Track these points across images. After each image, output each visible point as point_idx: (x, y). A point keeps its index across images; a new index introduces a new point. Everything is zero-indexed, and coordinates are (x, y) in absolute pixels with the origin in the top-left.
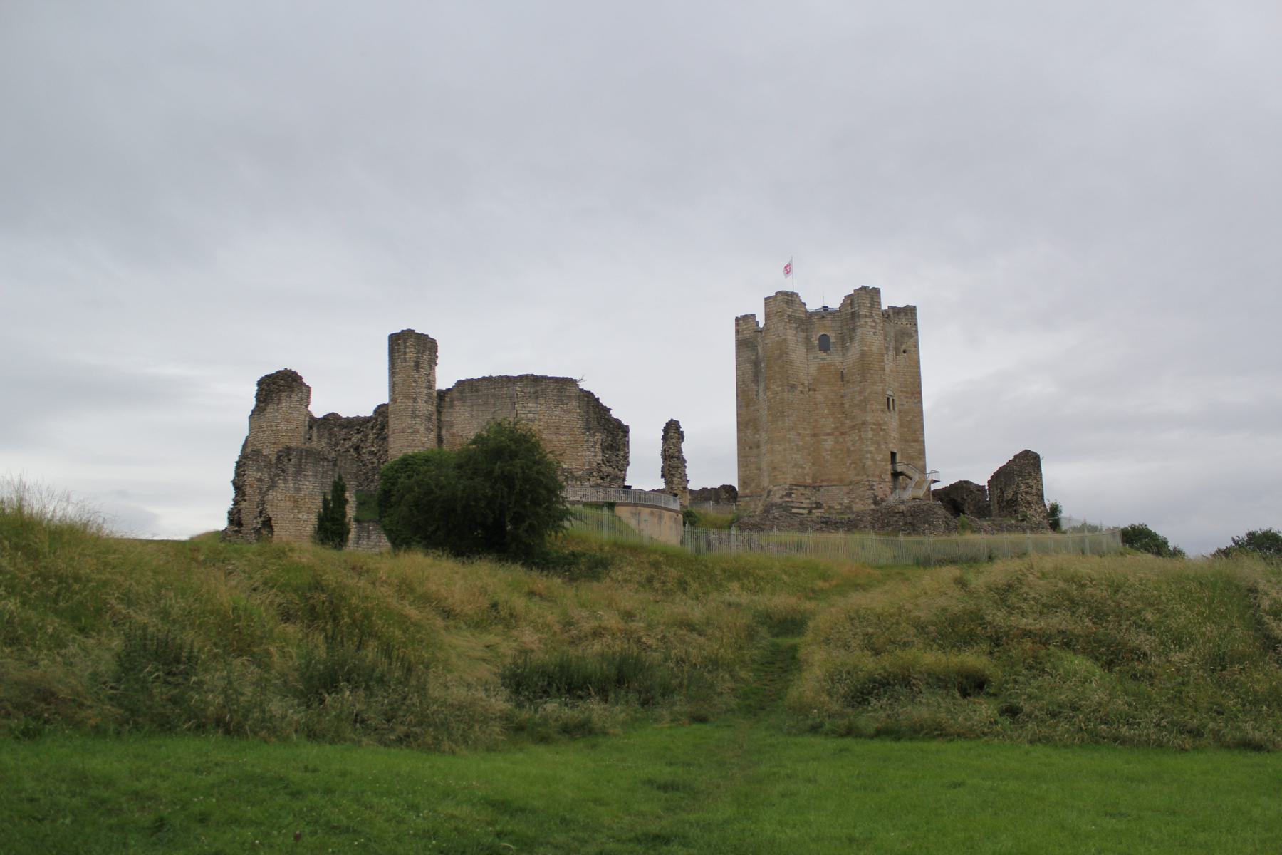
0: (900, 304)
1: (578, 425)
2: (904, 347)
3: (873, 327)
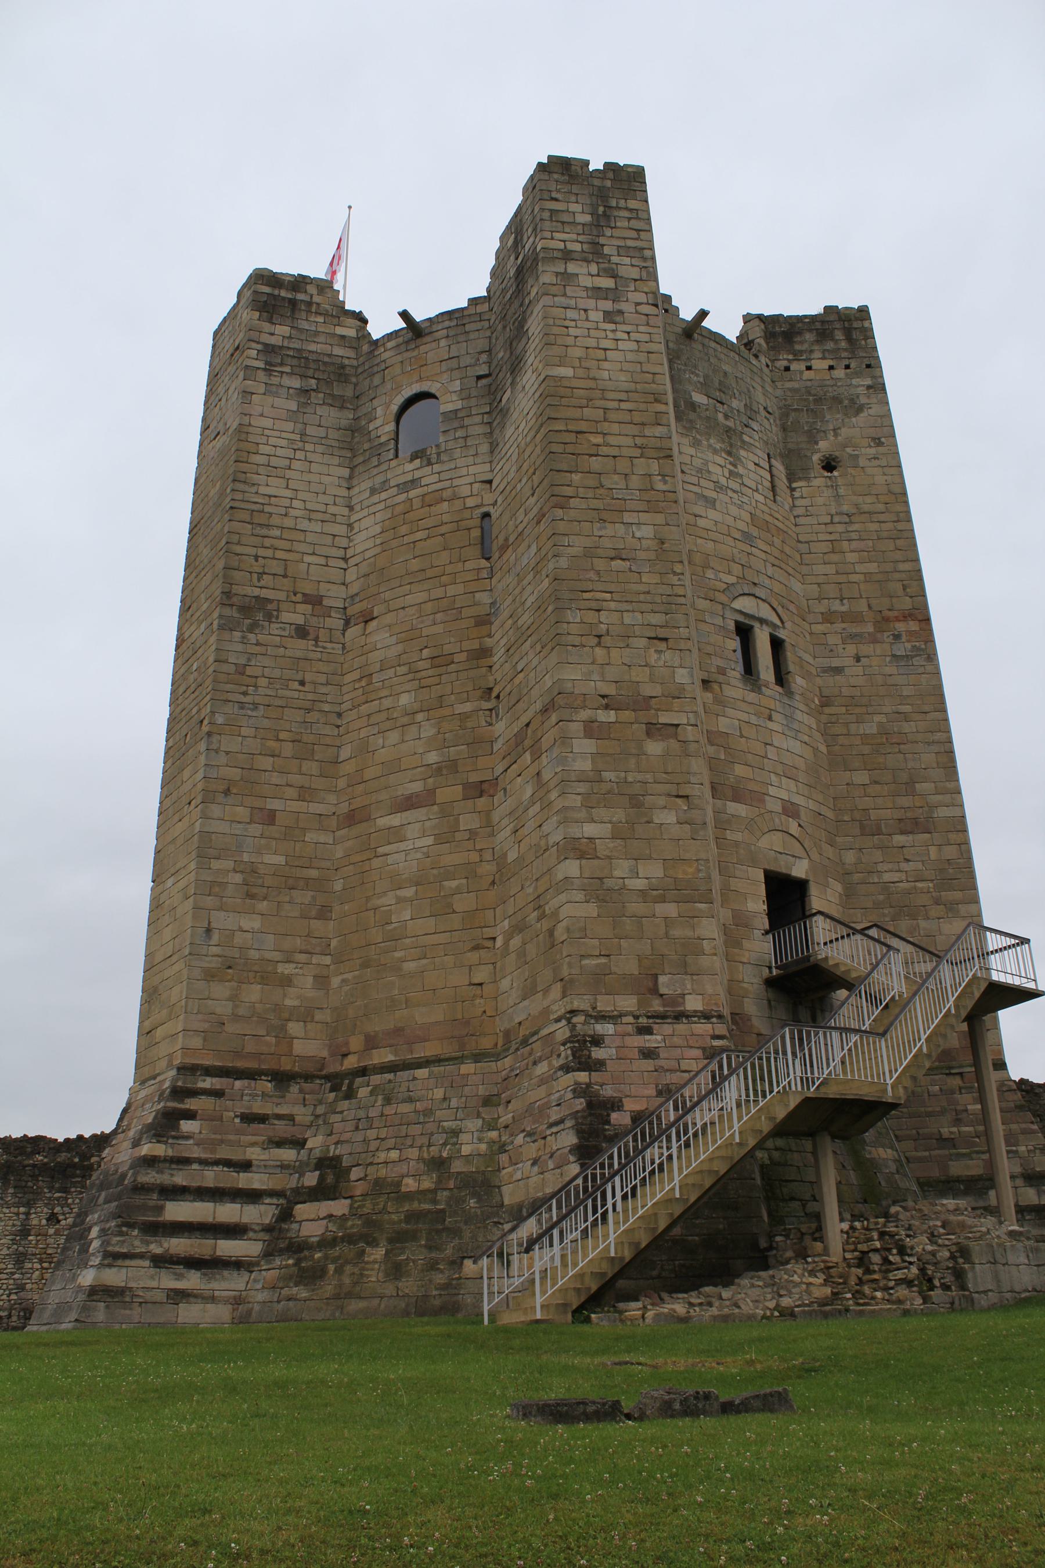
0: (803, 302)
2: (824, 446)
3: (597, 293)
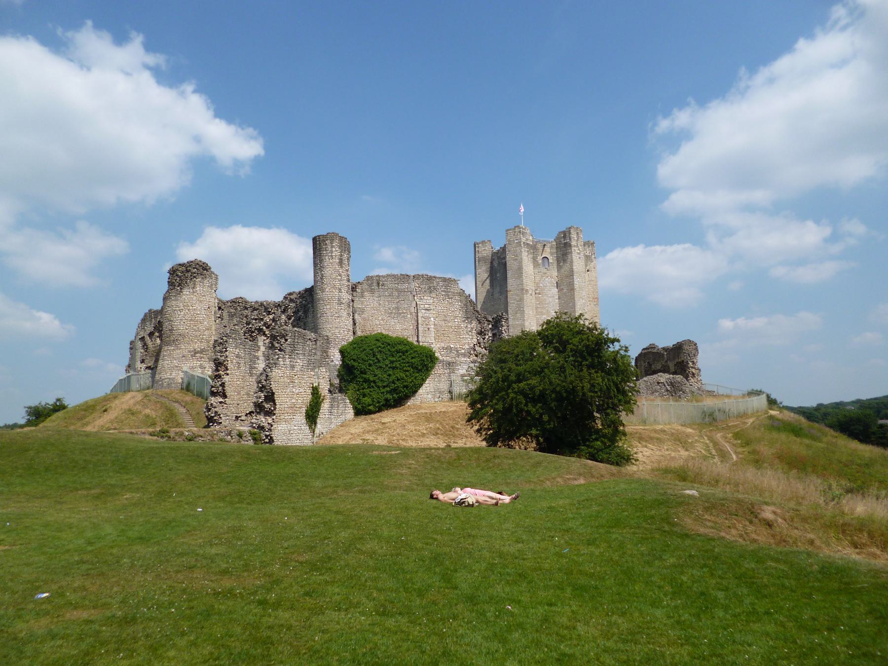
1: (460, 314)
